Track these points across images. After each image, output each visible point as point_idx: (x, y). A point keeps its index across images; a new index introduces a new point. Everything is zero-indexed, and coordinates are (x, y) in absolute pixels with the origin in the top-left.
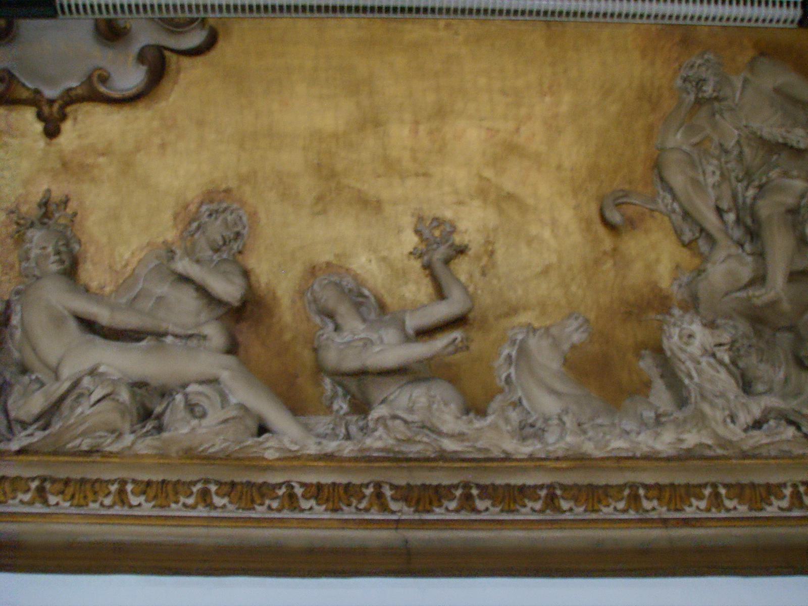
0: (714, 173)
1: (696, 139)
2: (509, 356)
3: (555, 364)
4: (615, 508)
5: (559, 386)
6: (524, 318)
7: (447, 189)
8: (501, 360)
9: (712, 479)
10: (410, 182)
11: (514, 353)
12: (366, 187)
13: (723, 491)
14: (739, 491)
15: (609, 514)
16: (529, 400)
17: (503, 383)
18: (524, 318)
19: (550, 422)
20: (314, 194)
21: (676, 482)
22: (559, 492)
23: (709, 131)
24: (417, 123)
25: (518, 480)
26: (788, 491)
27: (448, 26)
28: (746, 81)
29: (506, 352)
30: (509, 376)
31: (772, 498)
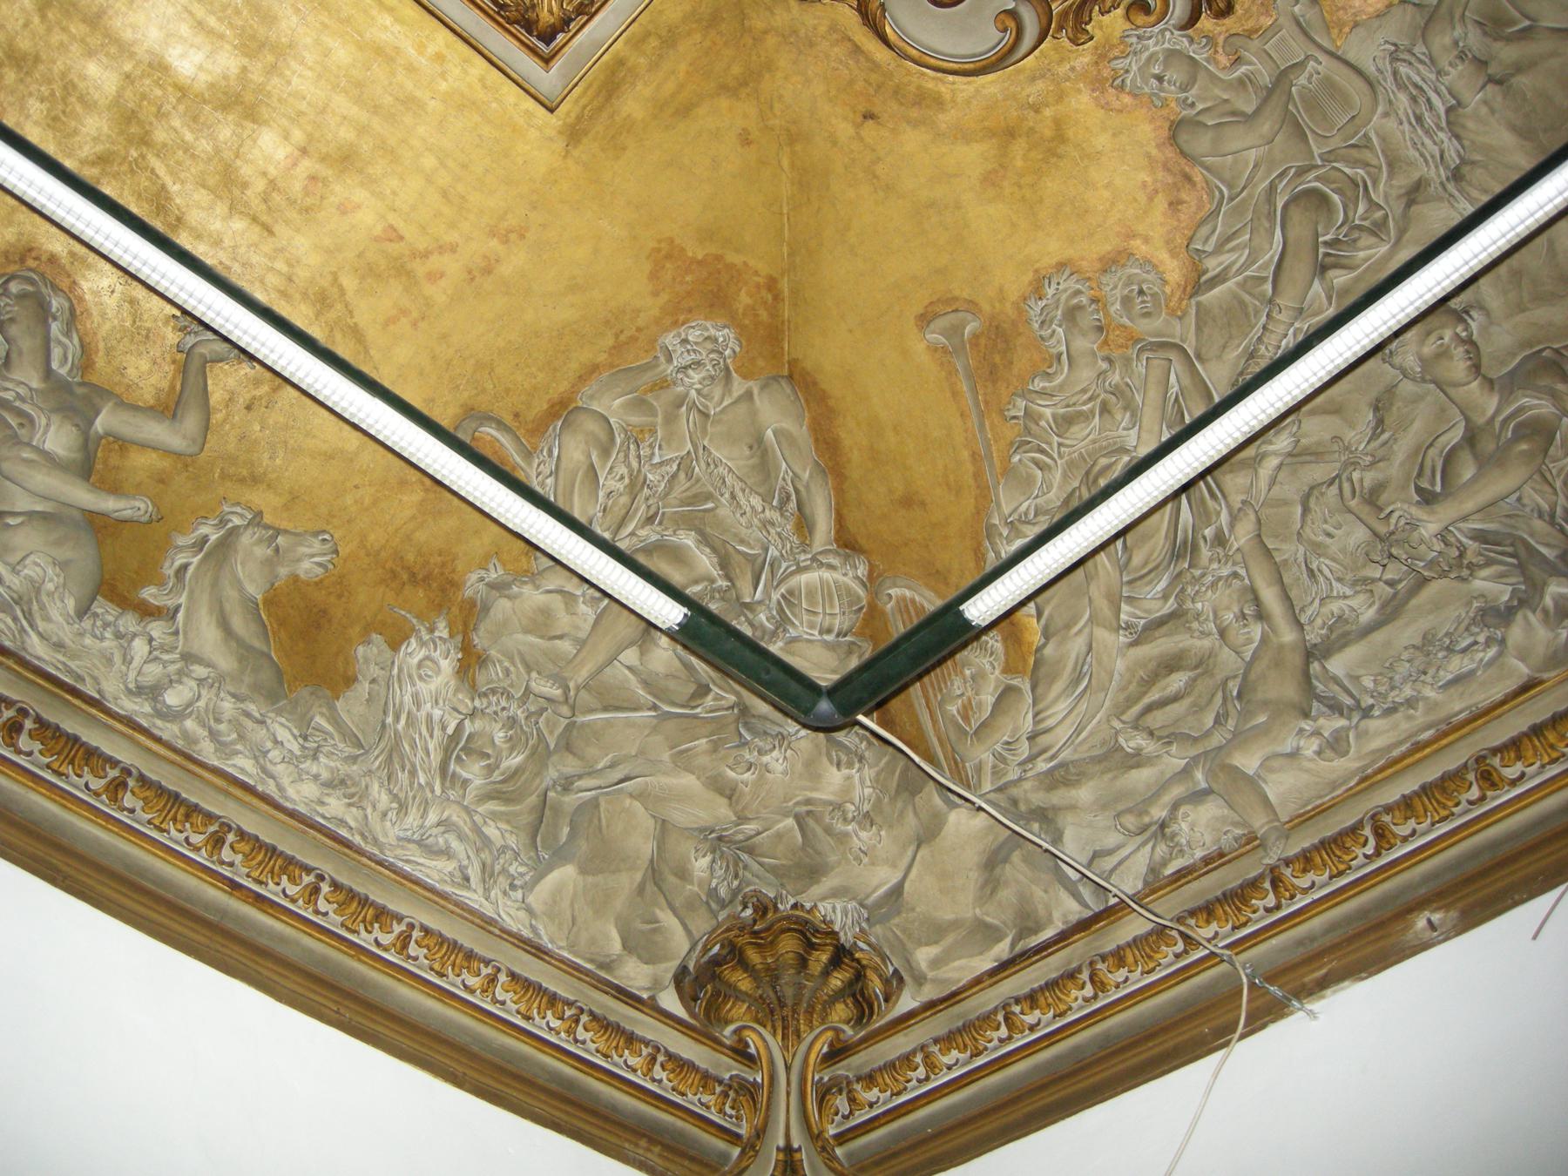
0: (622, 478)
1: (635, 419)
2: (205, 539)
3: (255, 590)
4: (187, 839)
5: (238, 623)
6: (259, 498)
7: (280, 265)
8: (189, 539)
9: (328, 868)
10: (238, 224)
11: (213, 538)
12: (174, 188)
13: (325, 888)
14: (348, 897)
15: (177, 842)
16: (188, 617)
17: (171, 572)
18: (259, 498)
19: (185, 679)
20: (99, 148)
21: (280, 848)
22: (131, 783)
23: (660, 419)
24: (304, 151)
25: (92, 737)
26: (398, 928)
27: (439, 58)
28: (748, 396)
29: (204, 530)
30: (185, 567)
31: (376, 925)
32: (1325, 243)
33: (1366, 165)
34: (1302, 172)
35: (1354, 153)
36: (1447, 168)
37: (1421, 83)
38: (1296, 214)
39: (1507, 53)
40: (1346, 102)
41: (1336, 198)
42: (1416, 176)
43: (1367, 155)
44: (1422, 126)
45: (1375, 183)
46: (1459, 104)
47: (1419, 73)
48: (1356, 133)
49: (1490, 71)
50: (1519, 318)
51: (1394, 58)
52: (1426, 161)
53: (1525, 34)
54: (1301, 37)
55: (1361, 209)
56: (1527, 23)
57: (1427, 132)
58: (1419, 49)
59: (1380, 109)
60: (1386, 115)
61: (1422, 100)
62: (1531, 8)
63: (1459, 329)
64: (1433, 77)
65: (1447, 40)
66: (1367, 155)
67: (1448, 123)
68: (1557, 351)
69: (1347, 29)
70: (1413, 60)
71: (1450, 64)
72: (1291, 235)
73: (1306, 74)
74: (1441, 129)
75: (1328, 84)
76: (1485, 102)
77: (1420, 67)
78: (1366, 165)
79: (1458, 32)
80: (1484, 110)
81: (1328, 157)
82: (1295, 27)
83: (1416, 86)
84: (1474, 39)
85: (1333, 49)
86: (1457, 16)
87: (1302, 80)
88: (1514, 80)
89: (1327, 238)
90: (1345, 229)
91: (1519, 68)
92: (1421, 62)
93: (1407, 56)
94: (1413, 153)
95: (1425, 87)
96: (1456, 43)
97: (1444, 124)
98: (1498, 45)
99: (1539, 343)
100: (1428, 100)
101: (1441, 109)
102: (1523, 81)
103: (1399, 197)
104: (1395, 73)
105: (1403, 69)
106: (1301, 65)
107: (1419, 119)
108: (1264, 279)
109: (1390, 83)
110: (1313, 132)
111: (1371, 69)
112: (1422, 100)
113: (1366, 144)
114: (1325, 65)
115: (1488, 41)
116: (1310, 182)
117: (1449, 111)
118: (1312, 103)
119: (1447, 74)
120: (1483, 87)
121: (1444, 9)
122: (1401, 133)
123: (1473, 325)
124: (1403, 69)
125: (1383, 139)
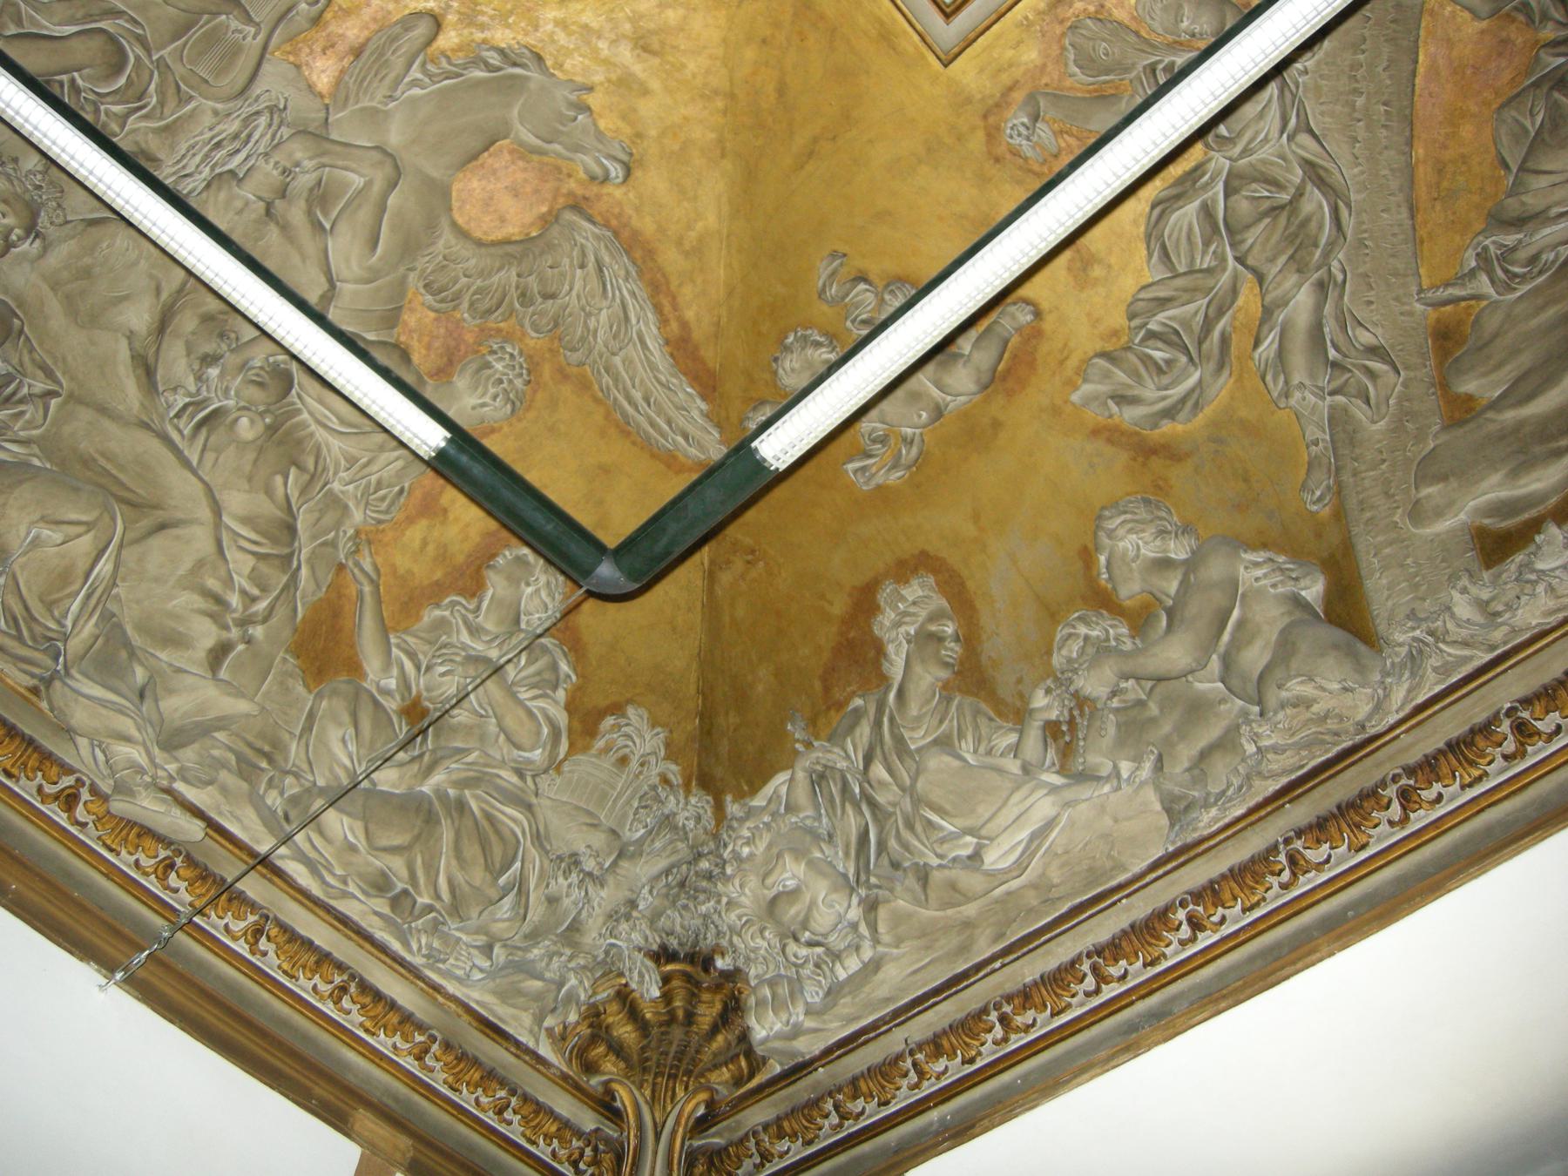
32: (73, 81)
33: (162, 103)
34: (142, 40)
35: (171, 91)
36: (175, 182)
37: (253, 140)
38: (96, 43)
39: (296, 214)
40: (221, 72)
41: (122, 81)
42: (161, 155)
43: (172, 103)
44: (211, 150)
45: (146, 117)
46: (240, 180)
47: (262, 136)
48: (191, 88)
49: (277, 202)
50: (45, 288)
51: (272, 109)
52: (178, 162)
53: (318, 227)
54: (275, 15)
55: (117, 109)
56: (328, 227)
57: (207, 156)
58: (285, 132)
59: (219, 106)
60: (216, 113)
61: (237, 145)
62: (342, 227)
63: (17, 231)
64: (262, 150)
65: (299, 155)
66: (172, 103)
67: (220, 175)
68: (21, 332)
69: (292, 58)
70: (274, 127)
71: (277, 163)
72: (75, 43)
73: (241, 27)
74: (212, 169)
75: (235, 51)
76: (247, 204)
77: (269, 136)
78: (162, 103)
79: (308, 164)
80: (239, 204)
81: (161, 65)
82: (284, 8)
83: (249, 136)
84: (304, 181)
85: (270, 48)
86: (325, 160)
87: (235, 24)
88: (272, 227)
89: (80, 82)
90: (91, 97)
91: (285, 228)
92: (274, 136)
93: (276, 120)
94: (183, 147)
95: (250, 145)
96: (297, 165)
97: (218, 171)
98: (302, 204)
99: (25, 313)
100: (238, 151)
101: (233, 164)
102: (273, 233)
103: (136, 143)
104: (257, 113)
105: (263, 121)
106: (249, 20)
107: (218, 145)
108: (19, 23)
109: (247, 110)
110: (185, 45)
111: (257, 89)
112: (237, 145)
113: (183, 100)
114: (253, 43)
115: (305, 195)
116: (133, 52)
117: (231, 171)
118: (213, 38)
119: (267, 162)
120: (260, 198)
121: (327, 146)
122: (201, 133)
123: (26, 246)
124: (263, 121)
125: (192, 115)
